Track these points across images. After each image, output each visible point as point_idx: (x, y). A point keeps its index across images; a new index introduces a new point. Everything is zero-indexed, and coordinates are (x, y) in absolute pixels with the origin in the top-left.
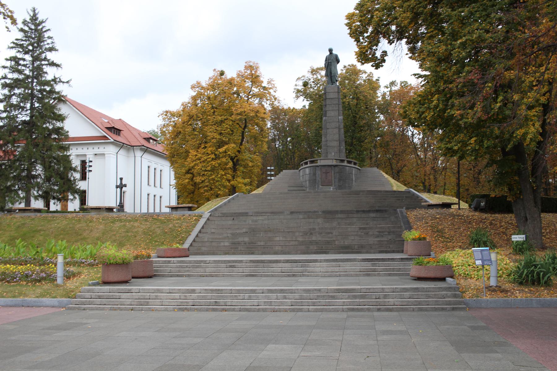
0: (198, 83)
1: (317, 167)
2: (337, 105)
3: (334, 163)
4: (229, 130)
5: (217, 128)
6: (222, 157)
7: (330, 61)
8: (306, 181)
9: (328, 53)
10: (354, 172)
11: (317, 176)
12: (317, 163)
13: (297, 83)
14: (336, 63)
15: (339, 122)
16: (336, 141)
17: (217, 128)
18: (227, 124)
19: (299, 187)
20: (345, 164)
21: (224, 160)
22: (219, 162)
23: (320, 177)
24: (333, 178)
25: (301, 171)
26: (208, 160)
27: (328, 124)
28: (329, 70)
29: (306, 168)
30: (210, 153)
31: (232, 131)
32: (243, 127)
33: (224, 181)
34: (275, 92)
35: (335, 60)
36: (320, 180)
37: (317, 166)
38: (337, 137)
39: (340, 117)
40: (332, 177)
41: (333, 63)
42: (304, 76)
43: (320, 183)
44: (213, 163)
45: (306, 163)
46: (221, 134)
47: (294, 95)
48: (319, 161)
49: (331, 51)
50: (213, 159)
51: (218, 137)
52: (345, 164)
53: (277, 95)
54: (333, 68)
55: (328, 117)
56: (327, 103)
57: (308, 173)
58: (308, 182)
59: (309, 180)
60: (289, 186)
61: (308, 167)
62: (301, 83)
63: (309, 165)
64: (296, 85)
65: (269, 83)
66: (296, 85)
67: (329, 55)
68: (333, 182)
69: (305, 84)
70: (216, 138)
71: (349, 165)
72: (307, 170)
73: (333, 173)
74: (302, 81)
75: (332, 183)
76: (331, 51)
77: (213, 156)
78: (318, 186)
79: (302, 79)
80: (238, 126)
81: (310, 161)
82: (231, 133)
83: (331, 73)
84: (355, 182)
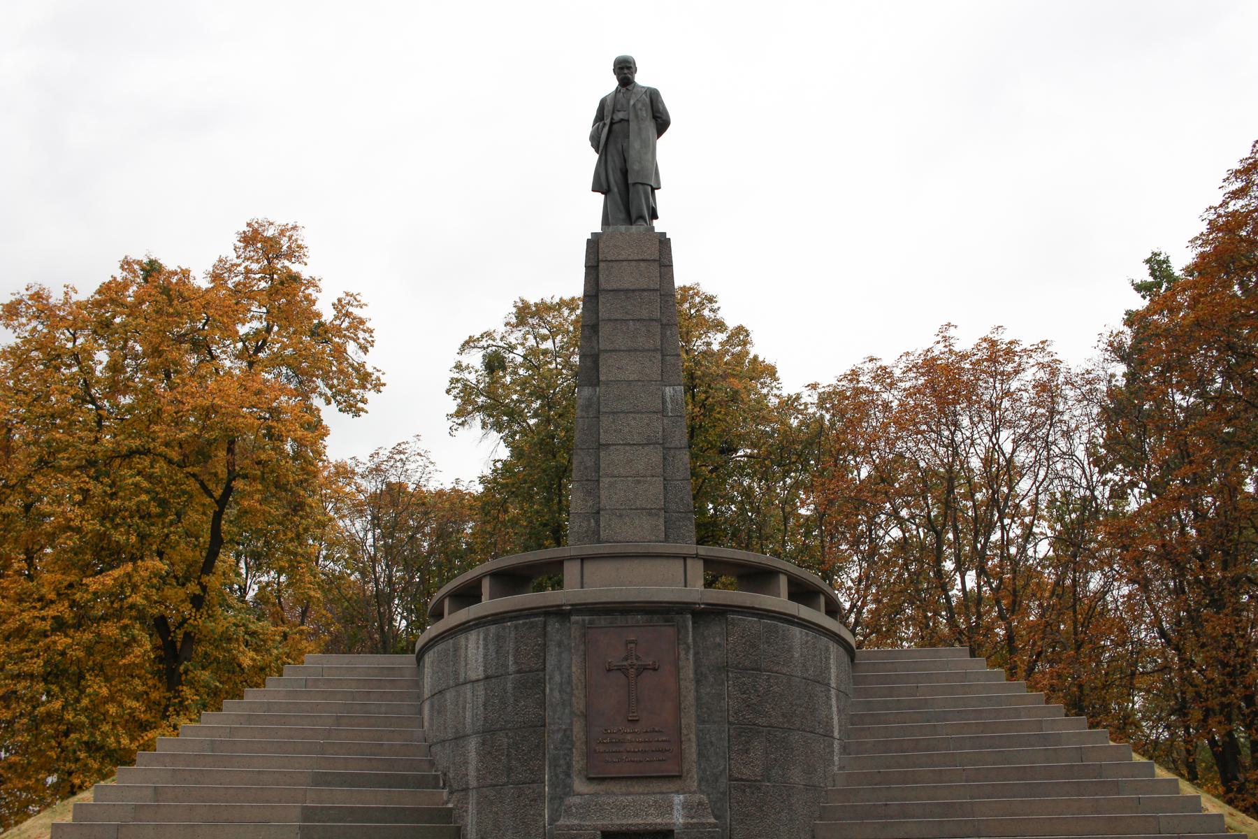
0: (38, 296)
1: (554, 626)
2: (656, 328)
3: (695, 590)
4: (144, 497)
5: (91, 485)
6: (104, 618)
7: (620, 115)
8: (459, 737)
9: (612, 84)
10: (833, 670)
11: (553, 694)
12: (559, 584)
13: (466, 359)
14: (651, 127)
15: (663, 412)
16: (650, 512)
17: (91, 485)
18: (139, 473)
19: (403, 782)
20: (779, 601)
21: (111, 630)
22: (88, 636)
23: (579, 704)
24: (689, 719)
25: (428, 659)
26: (39, 625)
27: (605, 421)
28: (615, 161)
29: (464, 628)
30: (53, 596)
31: (163, 503)
32: (218, 493)
33: (106, 728)
34: (365, 350)
35: (646, 114)
36: (578, 728)
37: (560, 613)
38: (652, 491)
39: (669, 391)
40: (678, 708)
41: (633, 126)
42: (488, 335)
43: (578, 762)
44: (61, 641)
45: (469, 594)
46: (106, 516)
47: (452, 405)
48: (571, 572)
49: (624, 69)
50: (60, 625)
51: (92, 526)
52: (779, 601)
53: (371, 361)
54: (635, 145)
55: (607, 383)
56: (603, 313)
57: (477, 671)
58: (473, 745)
59: (488, 733)
60: (320, 780)
61: (480, 622)
62: (475, 359)
63: (488, 604)
64: (459, 367)
65: (339, 306)
66: (459, 367)
67: (617, 91)
68: (691, 751)
69: (494, 363)
70: (78, 530)
71: (804, 612)
72: (474, 650)
73: (688, 672)
74: (484, 352)
75: (680, 757)
76: (624, 69)
77: (62, 609)
78: (563, 789)
79: (484, 343)
80: (192, 485)
81: (496, 575)
82: (155, 509)
83: (625, 173)
84: (845, 749)
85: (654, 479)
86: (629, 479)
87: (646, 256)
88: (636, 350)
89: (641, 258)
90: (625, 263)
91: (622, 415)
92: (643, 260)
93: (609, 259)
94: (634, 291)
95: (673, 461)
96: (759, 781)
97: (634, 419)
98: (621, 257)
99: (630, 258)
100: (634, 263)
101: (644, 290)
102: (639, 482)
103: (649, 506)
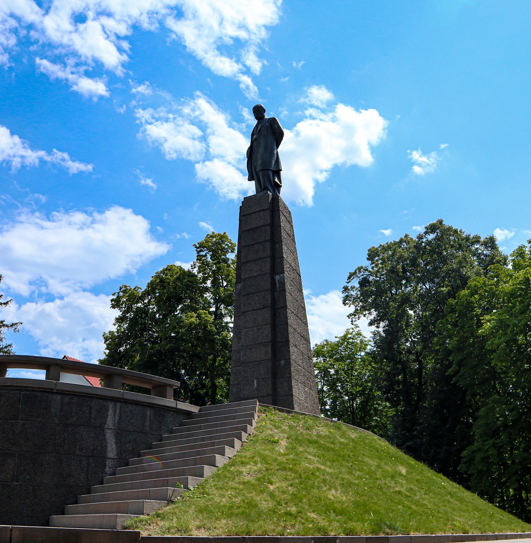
85: (267, 326)
86: (255, 328)
87: (263, 208)
88: (258, 259)
89: (260, 209)
90: (253, 214)
91: (251, 295)
92: (262, 210)
93: (246, 214)
94: (257, 228)
95: (279, 315)
96: (10, 482)
97: (257, 296)
98: (251, 212)
99: (256, 211)
100: (257, 214)
101: (263, 226)
102: (259, 329)
103: (264, 341)
